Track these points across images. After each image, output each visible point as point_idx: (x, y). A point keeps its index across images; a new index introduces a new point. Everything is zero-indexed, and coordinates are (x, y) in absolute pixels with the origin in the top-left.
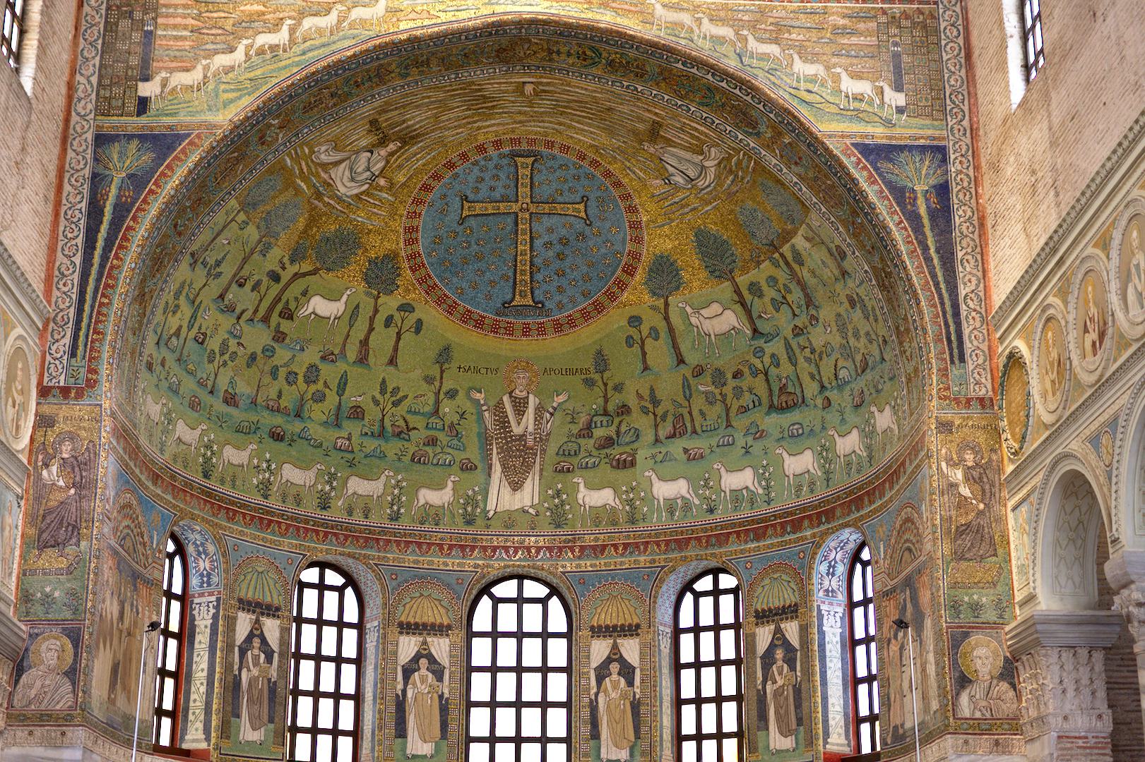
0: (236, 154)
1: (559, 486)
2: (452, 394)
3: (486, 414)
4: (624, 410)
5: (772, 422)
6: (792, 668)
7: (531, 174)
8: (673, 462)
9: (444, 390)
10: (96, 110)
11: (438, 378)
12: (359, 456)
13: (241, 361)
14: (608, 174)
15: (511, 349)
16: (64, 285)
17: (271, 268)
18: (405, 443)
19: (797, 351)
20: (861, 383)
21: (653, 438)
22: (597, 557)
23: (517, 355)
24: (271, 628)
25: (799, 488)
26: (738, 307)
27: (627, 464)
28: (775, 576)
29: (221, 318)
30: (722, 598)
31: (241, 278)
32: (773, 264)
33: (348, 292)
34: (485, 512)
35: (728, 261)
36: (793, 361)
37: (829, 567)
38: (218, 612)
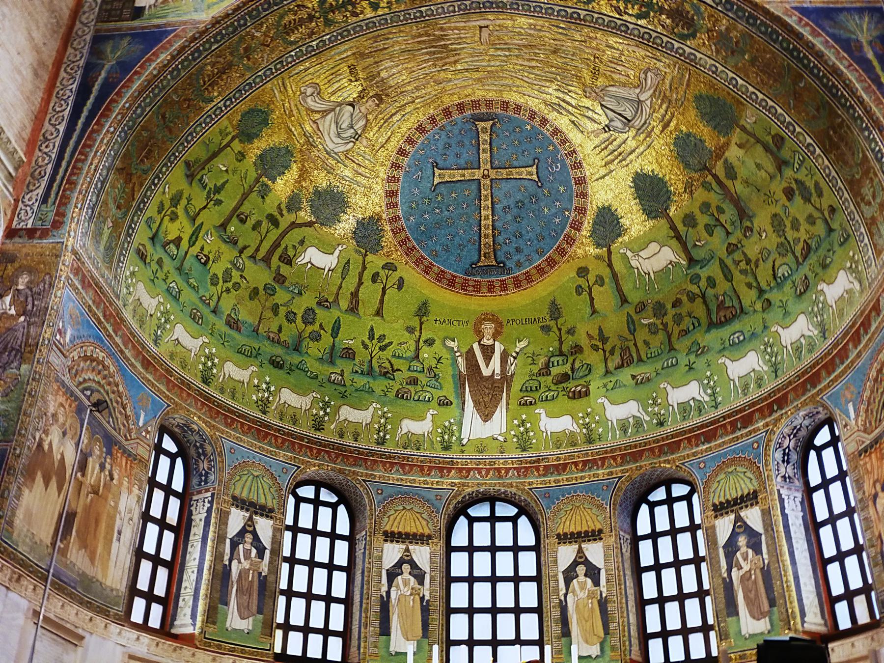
0: (221, 60)
1: (524, 417)
2: (430, 342)
3: (459, 359)
4: (577, 349)
5: (712, 338)
6: (757, 550)
7: (491, 139)
8: (623, 388)
9: (423, 339)
10: (97, 19)
11: (418, 329)
12: (350, 390)
13: (244, 293)
14: (556, 131)
15: (480, 305)
16: (46, 147)
17: (270, 211)
18: (390, 381)
19: (732, 267)
20: (805, 270)
21: (604, 370)
22: (559, 474)
23: (484, 309)
24: (264, 527)
25: (746, 387)
26: (674, 242)
27: (582, 394)
28: (730, 470)
29: (224, 247)
30: (676, 506)
31: (242, 214)
32: (706, 189)
33: (340, 248)
34: (460, 439)
35: (663, 199)
36: (728, 276)
37: (784, 454)
38: (211, 507)
